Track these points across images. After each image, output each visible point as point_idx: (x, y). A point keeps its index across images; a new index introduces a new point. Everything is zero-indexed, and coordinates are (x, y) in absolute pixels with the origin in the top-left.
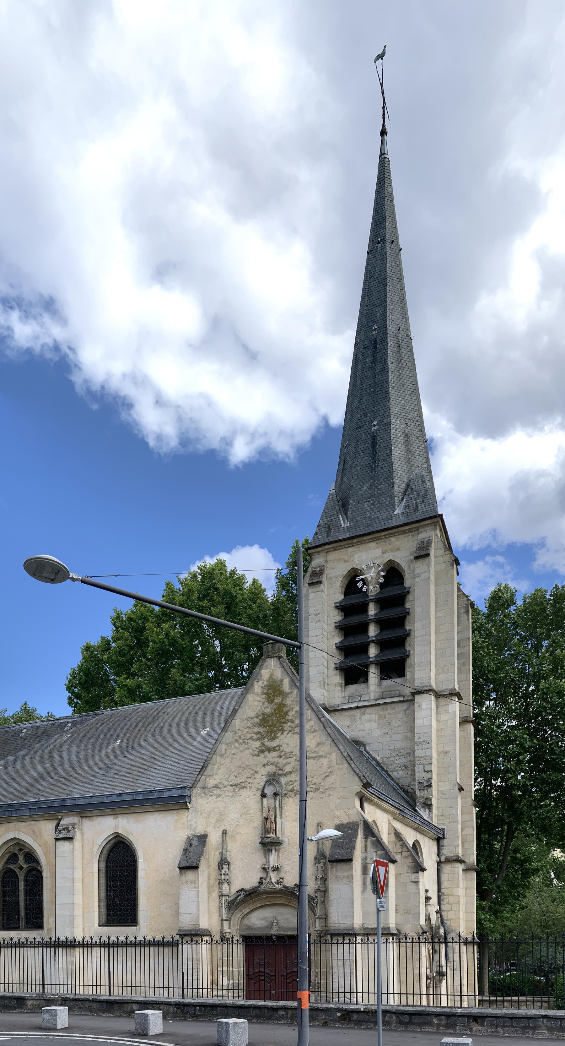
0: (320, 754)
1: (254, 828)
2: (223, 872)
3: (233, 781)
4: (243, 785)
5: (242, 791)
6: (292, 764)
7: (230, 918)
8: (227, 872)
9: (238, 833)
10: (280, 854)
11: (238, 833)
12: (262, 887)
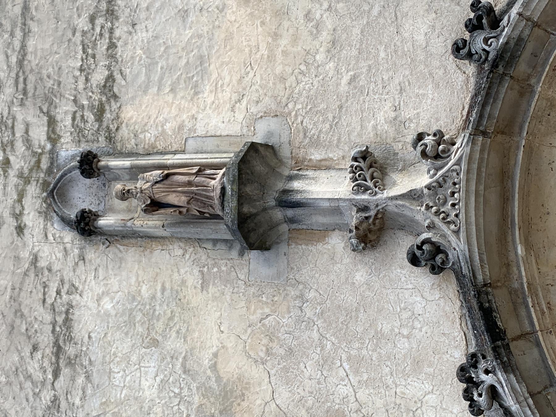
0: (18, 10)
1: (204, 286)
3: (46, 364)
4: (60, 320)
5: (80, 330)
6: (30, 119)
9: (214, 367)
10: (316, 156)
11: (214, 367)
12: (457, 246)
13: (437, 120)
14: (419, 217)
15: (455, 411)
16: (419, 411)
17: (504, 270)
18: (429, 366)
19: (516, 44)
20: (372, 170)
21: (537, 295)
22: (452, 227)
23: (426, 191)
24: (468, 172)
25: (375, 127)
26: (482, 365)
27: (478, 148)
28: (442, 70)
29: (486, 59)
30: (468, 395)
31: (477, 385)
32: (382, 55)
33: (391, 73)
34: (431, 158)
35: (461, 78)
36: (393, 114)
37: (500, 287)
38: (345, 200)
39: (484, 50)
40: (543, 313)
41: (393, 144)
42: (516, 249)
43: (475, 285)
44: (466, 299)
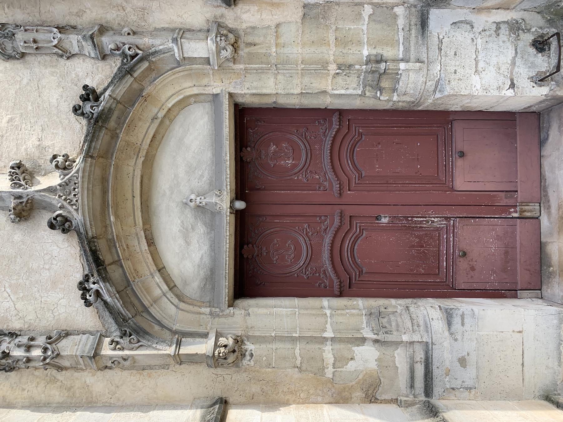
2: (18, 353)
7: (175, 332)
8: (24, 340)
13: (65, 148)
14: (54, 202)
15: (77, 306)
16: (56, 309)
17: (104, 229)
18: (61, 284)
19: (108, 111)
20: (24, 175)
21: (121, 241)
22: (74, 207)
23: (58, 187)
24: (83, 177)
25: (26, 150)
26: (92, 280)
27: (88, 165)
28: (67, 121)
29: (92, 117)
30: (83, 297)
31: (88, 291)
32: (30, 108)
33: (36, 119)
34: (61, 169)
35: (79, 126)
36: (38, 143)
37: (102, 238)
38: (6, 192)
39: (91, 112)
40: (124, 250)
41: (38, 160)
42: (110, 218)
43: (87, 238)
44: (83, 246)
